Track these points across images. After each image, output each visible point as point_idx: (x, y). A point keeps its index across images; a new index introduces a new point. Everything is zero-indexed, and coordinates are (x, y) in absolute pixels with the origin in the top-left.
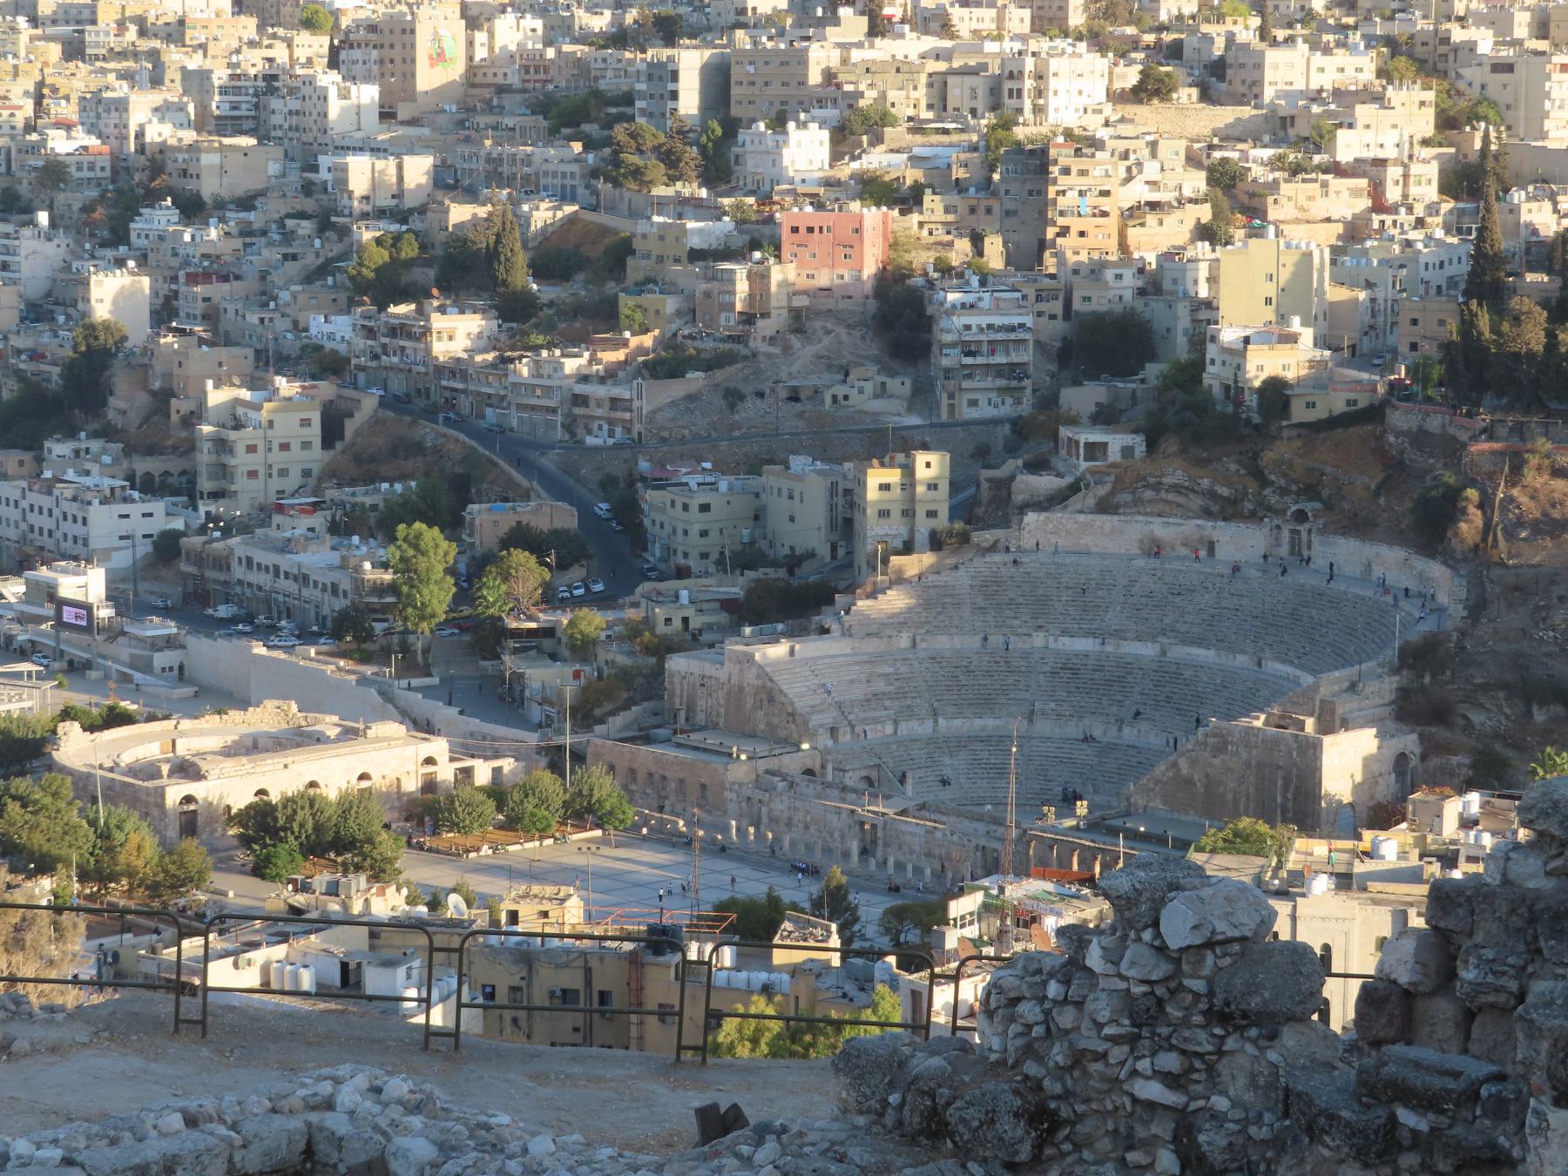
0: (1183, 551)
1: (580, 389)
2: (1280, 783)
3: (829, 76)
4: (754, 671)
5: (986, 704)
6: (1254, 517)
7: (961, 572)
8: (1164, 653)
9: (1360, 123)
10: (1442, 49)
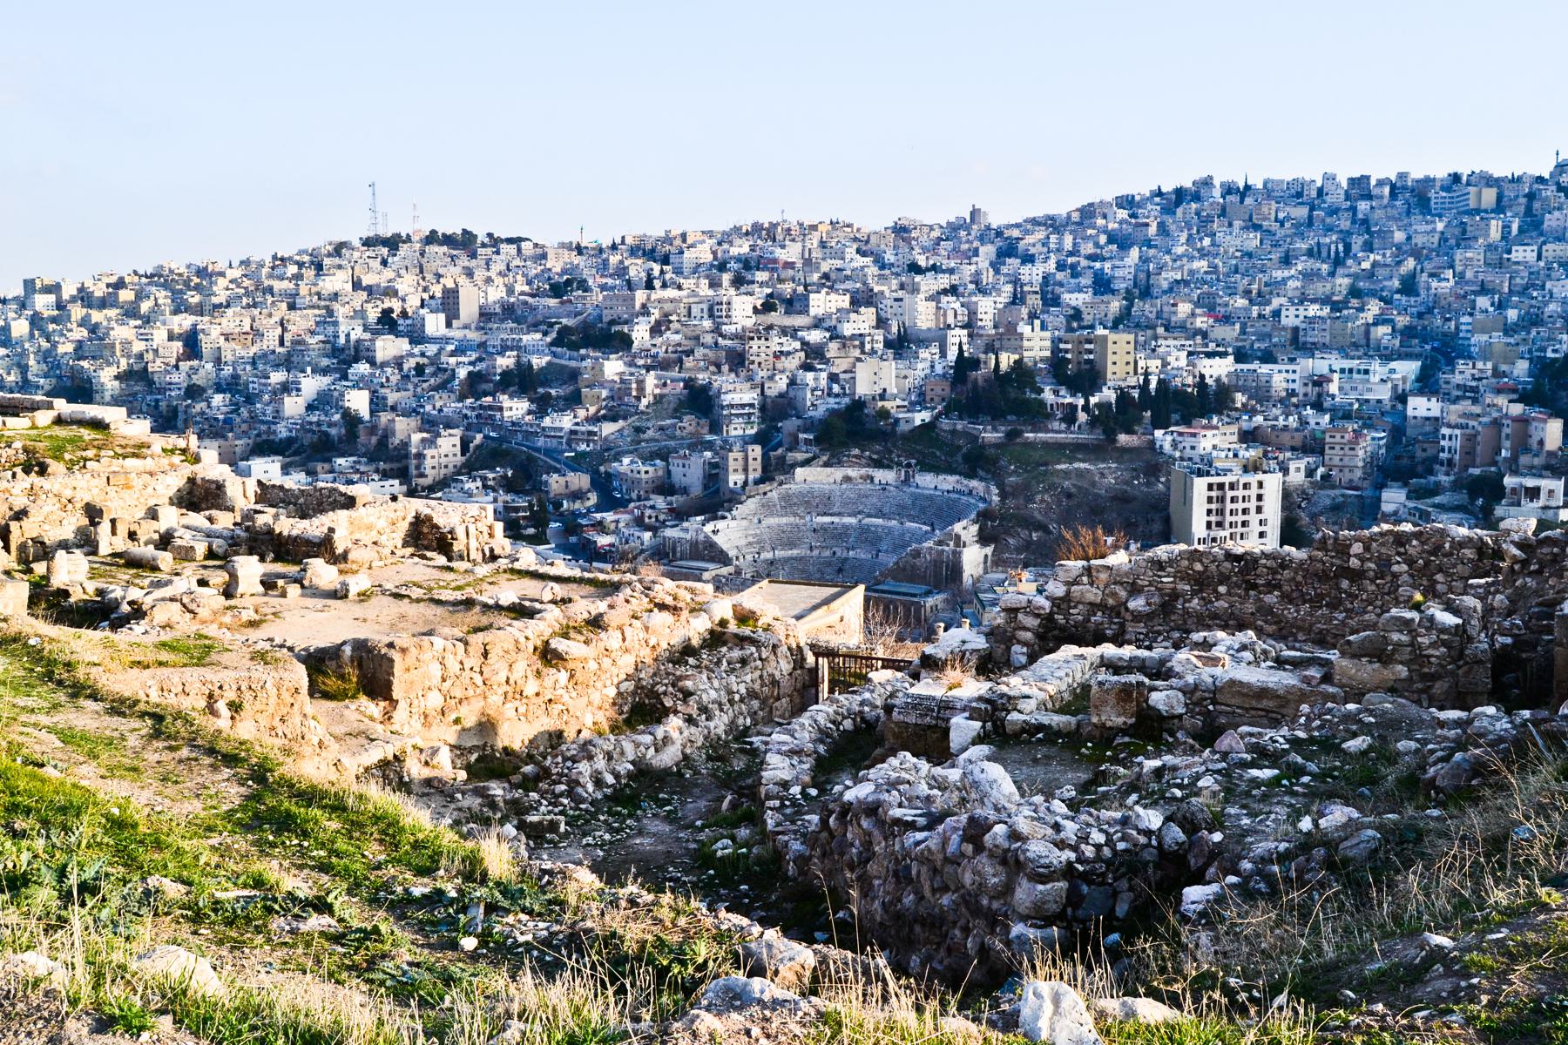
3: (644, 306)
5: (791, 544)
6: (889, 467)
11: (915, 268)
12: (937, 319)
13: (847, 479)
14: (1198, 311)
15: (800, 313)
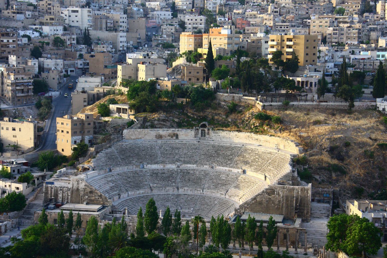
2: (294, 202)
7: (113, 148)
8: (178, 167)
10: (49, 6)
13: (160, 137)
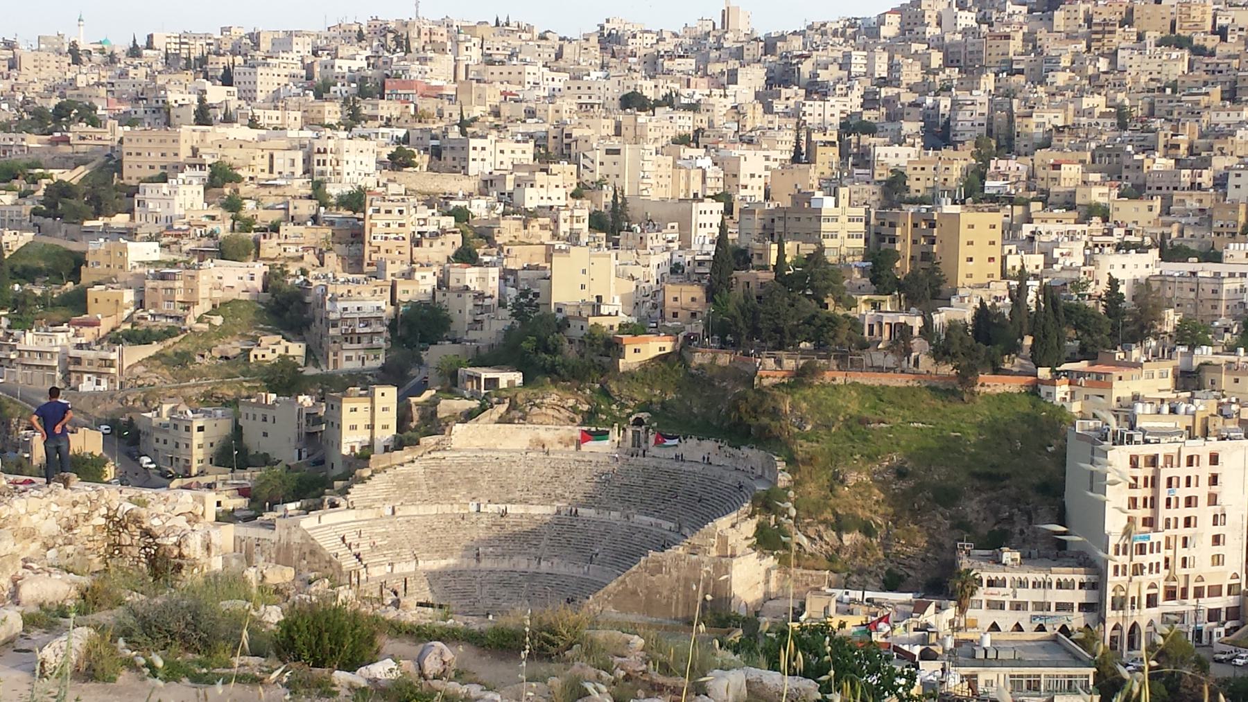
0: (559, 447)
1: (74, 353)
4: (299, 534)
9: (538, 184)
10: (566, 141)
11: (632, 101)
12: (676, 183)
14: (1095, 177)
15: (453, 170)
